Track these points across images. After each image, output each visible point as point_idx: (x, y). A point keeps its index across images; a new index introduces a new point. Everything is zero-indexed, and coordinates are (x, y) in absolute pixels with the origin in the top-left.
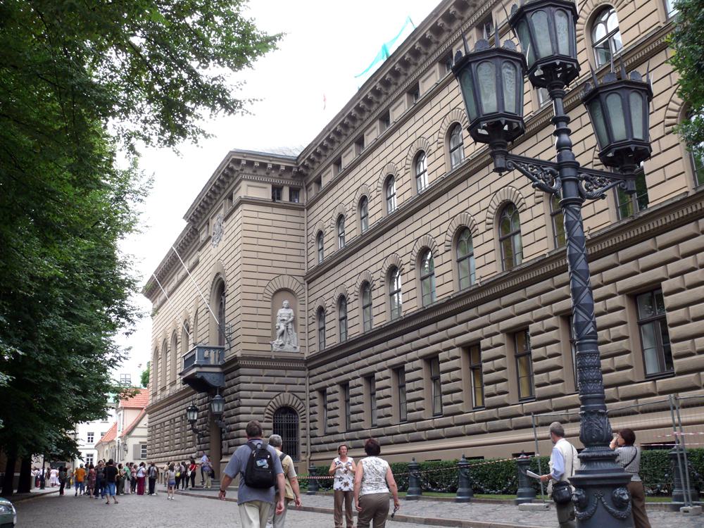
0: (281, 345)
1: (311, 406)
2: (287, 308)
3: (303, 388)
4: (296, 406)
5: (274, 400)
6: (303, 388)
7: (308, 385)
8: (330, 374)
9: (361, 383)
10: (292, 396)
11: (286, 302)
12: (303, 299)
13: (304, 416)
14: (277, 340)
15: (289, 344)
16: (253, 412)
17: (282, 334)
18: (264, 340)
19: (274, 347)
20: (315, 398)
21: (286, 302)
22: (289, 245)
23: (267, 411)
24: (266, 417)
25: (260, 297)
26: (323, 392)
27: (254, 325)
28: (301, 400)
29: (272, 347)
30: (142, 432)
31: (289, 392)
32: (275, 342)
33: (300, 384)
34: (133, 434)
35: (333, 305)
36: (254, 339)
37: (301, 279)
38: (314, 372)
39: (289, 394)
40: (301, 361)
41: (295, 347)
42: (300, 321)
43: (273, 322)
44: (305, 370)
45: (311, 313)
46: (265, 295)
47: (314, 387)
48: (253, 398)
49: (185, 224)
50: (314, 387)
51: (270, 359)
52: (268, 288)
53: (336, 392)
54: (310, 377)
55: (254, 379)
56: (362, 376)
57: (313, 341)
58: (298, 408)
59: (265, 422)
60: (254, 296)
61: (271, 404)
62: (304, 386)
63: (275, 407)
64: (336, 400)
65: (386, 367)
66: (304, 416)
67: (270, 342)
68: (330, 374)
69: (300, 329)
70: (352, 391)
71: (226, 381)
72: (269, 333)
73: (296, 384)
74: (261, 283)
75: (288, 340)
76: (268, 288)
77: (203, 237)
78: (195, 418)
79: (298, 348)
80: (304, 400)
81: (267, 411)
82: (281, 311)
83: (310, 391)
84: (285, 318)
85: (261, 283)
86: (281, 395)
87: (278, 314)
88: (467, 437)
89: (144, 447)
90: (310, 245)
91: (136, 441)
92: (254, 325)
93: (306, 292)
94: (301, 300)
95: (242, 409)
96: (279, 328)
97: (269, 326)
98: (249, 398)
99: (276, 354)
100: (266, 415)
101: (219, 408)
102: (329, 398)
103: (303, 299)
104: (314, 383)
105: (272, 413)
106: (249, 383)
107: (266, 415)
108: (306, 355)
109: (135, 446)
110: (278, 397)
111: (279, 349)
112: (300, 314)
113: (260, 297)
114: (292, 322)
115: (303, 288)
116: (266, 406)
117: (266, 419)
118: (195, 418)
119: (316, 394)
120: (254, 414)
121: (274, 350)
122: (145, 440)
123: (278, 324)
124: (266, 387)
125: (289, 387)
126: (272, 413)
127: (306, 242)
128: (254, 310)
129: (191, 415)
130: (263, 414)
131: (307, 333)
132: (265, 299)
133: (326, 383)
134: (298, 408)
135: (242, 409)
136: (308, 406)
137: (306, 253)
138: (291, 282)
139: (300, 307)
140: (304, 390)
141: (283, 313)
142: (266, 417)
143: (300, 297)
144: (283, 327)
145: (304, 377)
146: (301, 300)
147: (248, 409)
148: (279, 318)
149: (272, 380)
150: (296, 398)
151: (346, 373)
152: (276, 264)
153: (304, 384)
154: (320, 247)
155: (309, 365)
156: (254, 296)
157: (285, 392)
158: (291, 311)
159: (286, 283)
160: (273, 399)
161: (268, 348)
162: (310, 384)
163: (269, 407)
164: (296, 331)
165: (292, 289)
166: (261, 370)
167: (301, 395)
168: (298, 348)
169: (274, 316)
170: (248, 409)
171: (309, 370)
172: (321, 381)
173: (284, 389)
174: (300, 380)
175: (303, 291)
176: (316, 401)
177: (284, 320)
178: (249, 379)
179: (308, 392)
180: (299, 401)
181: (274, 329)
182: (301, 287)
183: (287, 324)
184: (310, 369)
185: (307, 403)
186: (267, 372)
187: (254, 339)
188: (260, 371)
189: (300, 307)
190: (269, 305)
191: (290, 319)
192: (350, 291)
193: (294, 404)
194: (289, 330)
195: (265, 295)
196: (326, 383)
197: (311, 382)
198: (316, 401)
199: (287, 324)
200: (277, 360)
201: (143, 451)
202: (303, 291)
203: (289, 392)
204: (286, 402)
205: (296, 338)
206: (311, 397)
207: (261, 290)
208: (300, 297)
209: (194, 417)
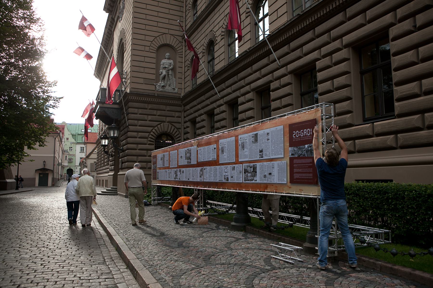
0: (163, 86)
1: (185, 134)
2: (169, 59)
3: (179, 120)
5: (156, 128)
6: (179, 120)
7: (183, 118)
8: (199, 106)
9: (224, 109)
10: (170, 126)
11: (168, 54)
12: (181, 53)
14: (160, 82)
15: (169, 86)
16: (139, 136)
17: (164, 78)
18: (148, 81)
19: (157, 88)
20: (188, 127)
21: (168, 54)
22: (172, 12)
23: (150, 136)
24: (150, 141)
25: (147, 49)
26: (194, 122)
27: (142, 70)
28: (178, 129)
29: (156, 87)
30: (94, 156)
31: (168, 122)
35: (204, 51)
36: (141, 81)
37: (180, 39)
38: (188, 107)
39: (168, 124)
40: (179, 99)
41: (174, 89)
42: (178, 70)
43: (157, 68)
44: (181, 107)
45: (186, 64)
46: (151, 48)
47: (187, 119)
48: (139, 126)
49: (106, 15)
50: (187, 119)
51: (153, 96)
52: (154, 42)
53: (203, 120)
54: (184, 112)
55: (140, 111)
56: (226, 103)
57: (188, 84)
58: (176, 135)
59: (149, 144)
60: (142, 48)
61: (154, 130)
63: (157, 134)
64: (204, 127)
65: (249, 90)
67: (154, 84)
68: (199, 106)
69: (178, 75)
70: (216, 118)
71: (122, 115)
72: (153, 77)
73: (174, 117)
74: (148, 38)
75: (169, 83)
76: (154, 42)
77: (116, 19)
78: (106, 144)
79: (176, 89)
81: (150, 136)
82: (163, 61)
83: (185, 122)
84: (167, 66)
85: (148, 38)
86: (162, 124)
87: (162, 63)
88: (356, 154)
89: (96, 164)
90: (187, 13)
91: (92, 161)
92: (142, 70)
93: (184, 48)
94: (179, 54)
95: (129, 134)
96: (162, 73)
97: (154, 71)
98: (136, 126)
99: (159, 93)
100: (149, 139)
101: (114, 134)
102: (198, 125)
103: (181, 53)
104: (188, 116)
105: (154, 138)
106: (137, 114)
107: (149, 139)
108: (182, 95)
109: (91, 164)
110: (159, 126)
111: (161, 89)
112: (178, 65)
113: (147, 49)
114: (172, 69)
115: (182, 45)
116: (149, 132)
118: (106, 144)
119: (188, 124)
120: (139, 138)
121: (157, 89)
122: (96, 160)
123: (161, 71)
124: (150, 118)
125: (168, 119)
126: (154, 138)
127: (184, 11)
128: (142, 59)
129: (103, 141)
130: (147, 138)
131: (183, 78)
132: (151, 51)
133: (196, 114)
134: (176, 135)
135: (129, 134)
136: (183, 134)
137: (184, 19)
138: (172, 40)
139: (179, 59)
141: (165, 62)
142: (150, 141)
143: (179, 51)
144: (164, 73)
145: (180, 112)
146: (179, 54)
147: (135, 134)
148: (162, 66)
149: (155, 112)
150: (173, 128)
151: (212, 103)
152: (160, 25)
153: (180, 117)
154: (195, 12)
155: (184, 102)
156: (142, 48)
157: (165, 122)
158: (171, 61)
159: (169, 40)
160: (155, 127)
161: (152, 88)
162: (185, 117)
163: (152, 133)
164: (175, 77)
166: (146, 105)
167: (178, 125)
168: (176, 89)
169: (158, 64)
170: (135, 134)
171: (184, 106)
172: (192, 114)
173: (164, 120)
174: (177, 114)
175: (181, 47)
176: (188, 130)
177: (166, 67)
178: (136, 111)
180: (176, 130)
181: (158, 74)
182: (180, 45)
183: (169, 70)
184: (185, 105)
185: (182, 131)
186: (150, 106)
187: (141, 81)
188: (146, 105)
189: (179, 59)
190: (154, 55)
191: (170, 68)
192: (218, 33)
193: (171, 131)
194: (170, 76)
195: (151, 48)
196: (196, 114)
197: (185, 116)
198: (188, 130)
199: (169, 70)
200: (159, 97)
201: (96, 167)
202: (181, 47)
203: (168, 122)
204: (166, 130)
205: (175, 83)
206: (185, 127)
207: (148, 44)
208: (179, 51)
209: (105, 143)
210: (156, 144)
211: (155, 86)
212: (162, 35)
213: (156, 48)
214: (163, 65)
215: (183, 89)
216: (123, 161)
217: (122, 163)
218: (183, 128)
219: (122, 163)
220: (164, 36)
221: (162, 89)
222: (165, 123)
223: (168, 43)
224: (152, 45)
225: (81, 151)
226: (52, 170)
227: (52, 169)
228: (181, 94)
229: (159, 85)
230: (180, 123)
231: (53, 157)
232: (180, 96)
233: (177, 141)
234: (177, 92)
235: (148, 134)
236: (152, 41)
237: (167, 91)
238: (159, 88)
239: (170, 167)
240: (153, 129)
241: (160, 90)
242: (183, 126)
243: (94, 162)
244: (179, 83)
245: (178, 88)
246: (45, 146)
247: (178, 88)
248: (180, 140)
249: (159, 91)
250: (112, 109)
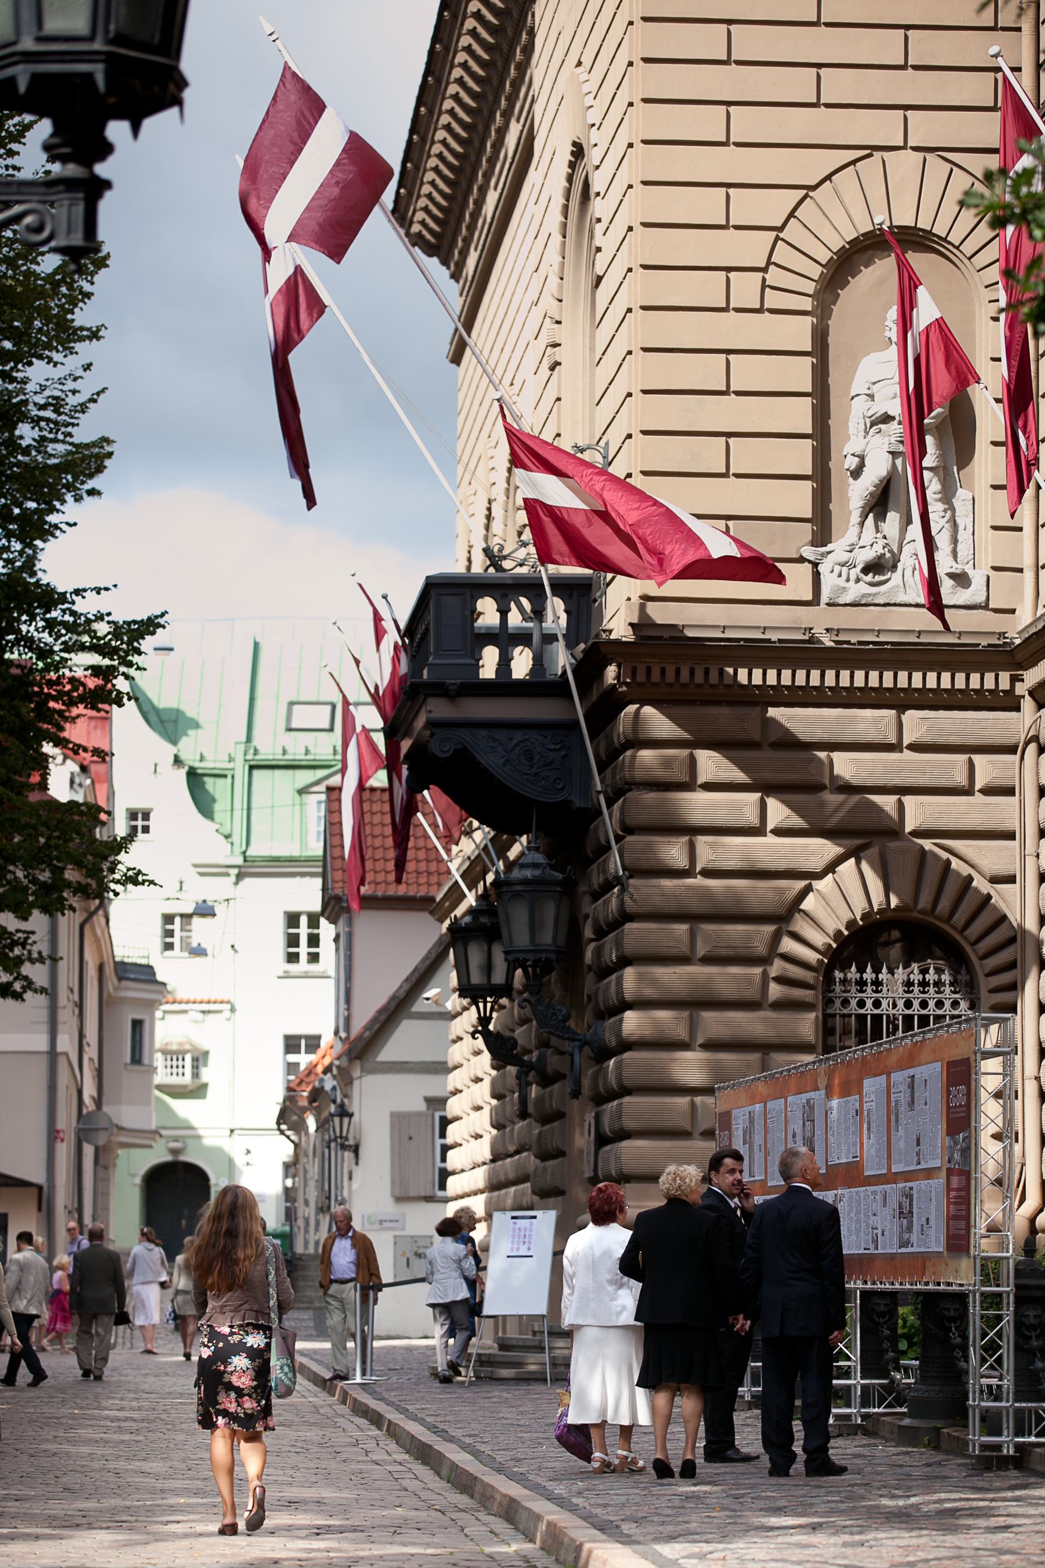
4: (960, 917)
5: (824, 885)
13: (1005, 978)
16: (701, 951)
24: (780, 980)
32: (838, 548)
33: (989, 791)
34: (391, 1050)
46: (774, 276)
59: (779, 1005)
62: (1014, 800)
66: (1005, 978)
67: (808, 552)
80: (1011, 879)
100: (777, 967)
101: (534, 926)
109: (400, 1121)
111: (855, 591)
117: (775, 990)
130: (763, 961)
132: (773, 299)
140: (1014, 825)
153: (1009, 791)
165: (924, 224)
168: (978, 579)
179: (1031, 831)
210: (828, 1002)
211: (815, 565)
212: (854, 162)
213: (816, 272)
214: (871, 397)
215: (1029, 575)
216: (607, 1128)
217: (602, 1140)
218: (1031, 878)
219: (602, 1140)
220: (870, 168)
221: (863, 589)
222: (892, 844)
223: (904, 218)
224: (782, 256)
225: (293, 958)
226: (40, 1188)
227: (37, 1175)
228: (1013, 611)
229: (844, 557)
230: (1010, 836)
231: (43, 1063)
232: (1002, 635)
233: (989, 975)
234: (981, 598)
235: (769, 929)
236: (779, 225)
237: (901, 598)
238: (841, 582)
239: (770, 1184)
240: (808, 889)
241: (847, 598)
242: (1030, 861)
243: (422, 1107)
244: (995, 528)
245: (995, 569)
246: (28, 995)
247: (995, 569)
248: (1012, 965)
249: (841, 601)
250: (519, 736)
